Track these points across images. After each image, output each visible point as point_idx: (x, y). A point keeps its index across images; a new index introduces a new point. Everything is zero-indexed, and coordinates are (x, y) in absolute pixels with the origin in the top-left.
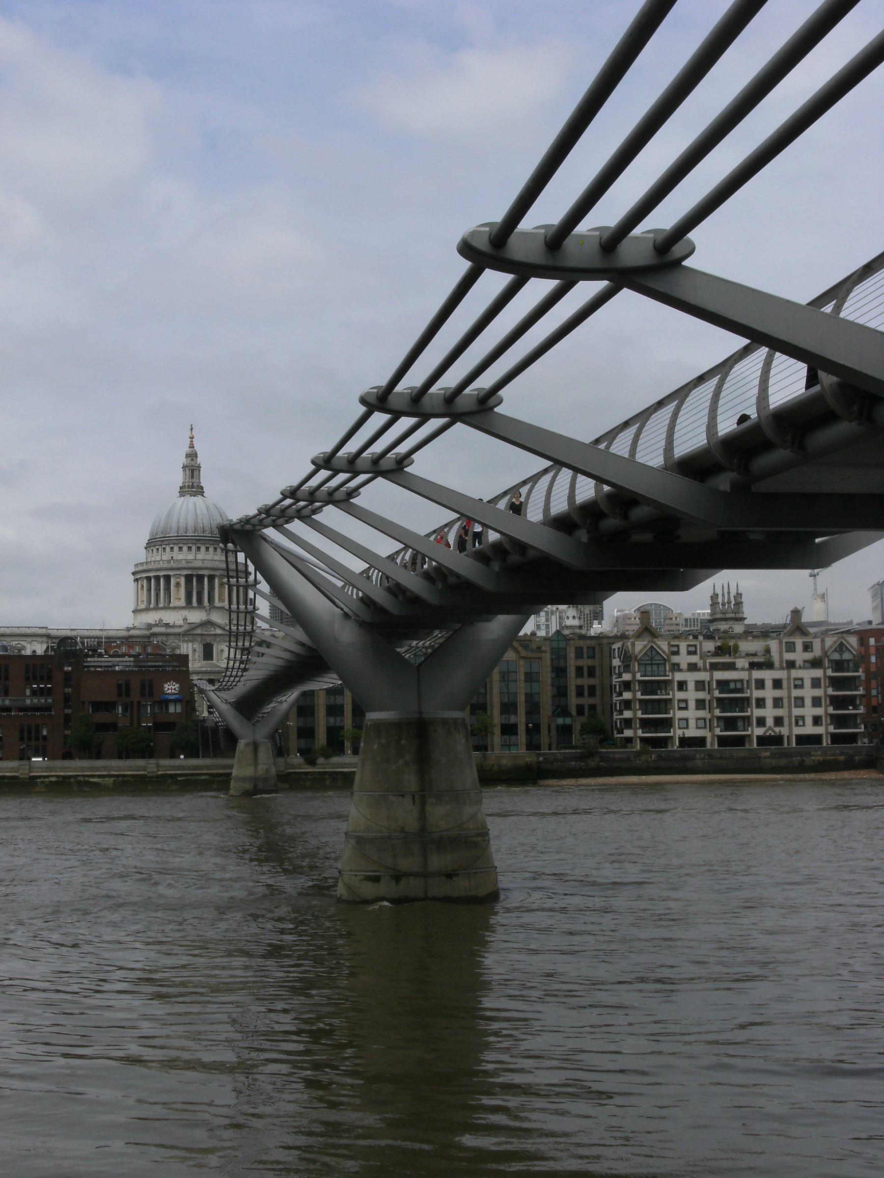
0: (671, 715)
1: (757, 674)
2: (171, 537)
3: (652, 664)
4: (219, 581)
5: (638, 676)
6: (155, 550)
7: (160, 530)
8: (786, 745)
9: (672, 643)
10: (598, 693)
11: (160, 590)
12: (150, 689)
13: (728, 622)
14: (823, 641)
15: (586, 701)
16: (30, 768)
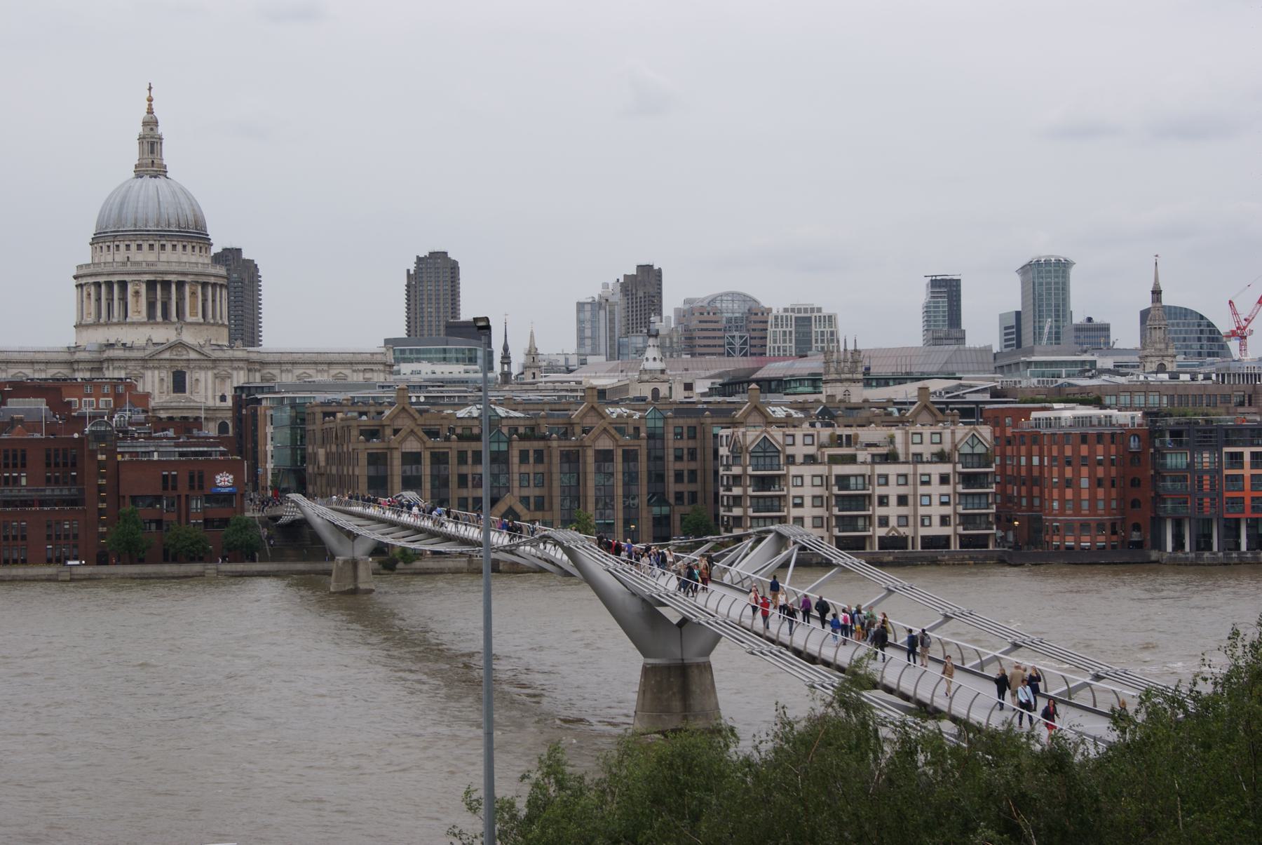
0: (785, 514)
1: (881, 469)
2: (126, 231)
3: (765, 457)
4: (190, 288)
5: (750, 471)
6: (105, 248)
7: (111, 222)
8: (910, 549)
9: (787, 433)
10: (699, 478)
11: (113, 300)
12: (199, 480)
13: (847, 384)
14: (953, 433)
15: (685, 487)
16: (71, 575)
